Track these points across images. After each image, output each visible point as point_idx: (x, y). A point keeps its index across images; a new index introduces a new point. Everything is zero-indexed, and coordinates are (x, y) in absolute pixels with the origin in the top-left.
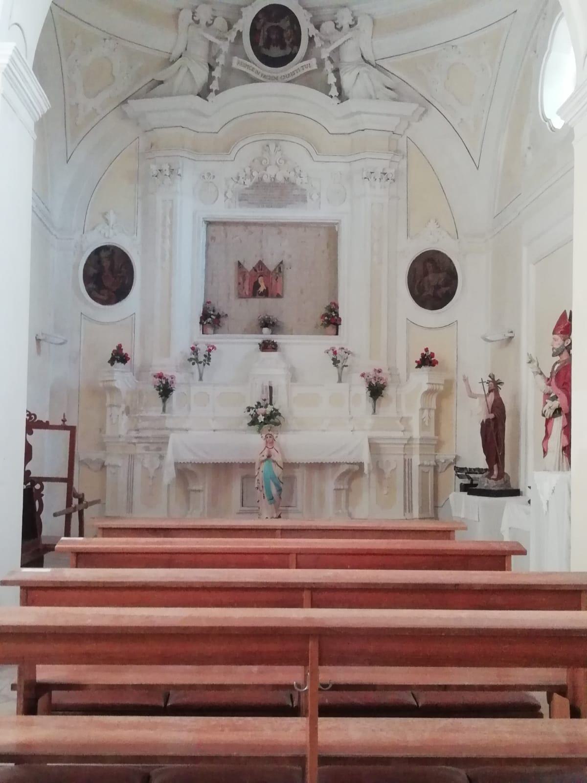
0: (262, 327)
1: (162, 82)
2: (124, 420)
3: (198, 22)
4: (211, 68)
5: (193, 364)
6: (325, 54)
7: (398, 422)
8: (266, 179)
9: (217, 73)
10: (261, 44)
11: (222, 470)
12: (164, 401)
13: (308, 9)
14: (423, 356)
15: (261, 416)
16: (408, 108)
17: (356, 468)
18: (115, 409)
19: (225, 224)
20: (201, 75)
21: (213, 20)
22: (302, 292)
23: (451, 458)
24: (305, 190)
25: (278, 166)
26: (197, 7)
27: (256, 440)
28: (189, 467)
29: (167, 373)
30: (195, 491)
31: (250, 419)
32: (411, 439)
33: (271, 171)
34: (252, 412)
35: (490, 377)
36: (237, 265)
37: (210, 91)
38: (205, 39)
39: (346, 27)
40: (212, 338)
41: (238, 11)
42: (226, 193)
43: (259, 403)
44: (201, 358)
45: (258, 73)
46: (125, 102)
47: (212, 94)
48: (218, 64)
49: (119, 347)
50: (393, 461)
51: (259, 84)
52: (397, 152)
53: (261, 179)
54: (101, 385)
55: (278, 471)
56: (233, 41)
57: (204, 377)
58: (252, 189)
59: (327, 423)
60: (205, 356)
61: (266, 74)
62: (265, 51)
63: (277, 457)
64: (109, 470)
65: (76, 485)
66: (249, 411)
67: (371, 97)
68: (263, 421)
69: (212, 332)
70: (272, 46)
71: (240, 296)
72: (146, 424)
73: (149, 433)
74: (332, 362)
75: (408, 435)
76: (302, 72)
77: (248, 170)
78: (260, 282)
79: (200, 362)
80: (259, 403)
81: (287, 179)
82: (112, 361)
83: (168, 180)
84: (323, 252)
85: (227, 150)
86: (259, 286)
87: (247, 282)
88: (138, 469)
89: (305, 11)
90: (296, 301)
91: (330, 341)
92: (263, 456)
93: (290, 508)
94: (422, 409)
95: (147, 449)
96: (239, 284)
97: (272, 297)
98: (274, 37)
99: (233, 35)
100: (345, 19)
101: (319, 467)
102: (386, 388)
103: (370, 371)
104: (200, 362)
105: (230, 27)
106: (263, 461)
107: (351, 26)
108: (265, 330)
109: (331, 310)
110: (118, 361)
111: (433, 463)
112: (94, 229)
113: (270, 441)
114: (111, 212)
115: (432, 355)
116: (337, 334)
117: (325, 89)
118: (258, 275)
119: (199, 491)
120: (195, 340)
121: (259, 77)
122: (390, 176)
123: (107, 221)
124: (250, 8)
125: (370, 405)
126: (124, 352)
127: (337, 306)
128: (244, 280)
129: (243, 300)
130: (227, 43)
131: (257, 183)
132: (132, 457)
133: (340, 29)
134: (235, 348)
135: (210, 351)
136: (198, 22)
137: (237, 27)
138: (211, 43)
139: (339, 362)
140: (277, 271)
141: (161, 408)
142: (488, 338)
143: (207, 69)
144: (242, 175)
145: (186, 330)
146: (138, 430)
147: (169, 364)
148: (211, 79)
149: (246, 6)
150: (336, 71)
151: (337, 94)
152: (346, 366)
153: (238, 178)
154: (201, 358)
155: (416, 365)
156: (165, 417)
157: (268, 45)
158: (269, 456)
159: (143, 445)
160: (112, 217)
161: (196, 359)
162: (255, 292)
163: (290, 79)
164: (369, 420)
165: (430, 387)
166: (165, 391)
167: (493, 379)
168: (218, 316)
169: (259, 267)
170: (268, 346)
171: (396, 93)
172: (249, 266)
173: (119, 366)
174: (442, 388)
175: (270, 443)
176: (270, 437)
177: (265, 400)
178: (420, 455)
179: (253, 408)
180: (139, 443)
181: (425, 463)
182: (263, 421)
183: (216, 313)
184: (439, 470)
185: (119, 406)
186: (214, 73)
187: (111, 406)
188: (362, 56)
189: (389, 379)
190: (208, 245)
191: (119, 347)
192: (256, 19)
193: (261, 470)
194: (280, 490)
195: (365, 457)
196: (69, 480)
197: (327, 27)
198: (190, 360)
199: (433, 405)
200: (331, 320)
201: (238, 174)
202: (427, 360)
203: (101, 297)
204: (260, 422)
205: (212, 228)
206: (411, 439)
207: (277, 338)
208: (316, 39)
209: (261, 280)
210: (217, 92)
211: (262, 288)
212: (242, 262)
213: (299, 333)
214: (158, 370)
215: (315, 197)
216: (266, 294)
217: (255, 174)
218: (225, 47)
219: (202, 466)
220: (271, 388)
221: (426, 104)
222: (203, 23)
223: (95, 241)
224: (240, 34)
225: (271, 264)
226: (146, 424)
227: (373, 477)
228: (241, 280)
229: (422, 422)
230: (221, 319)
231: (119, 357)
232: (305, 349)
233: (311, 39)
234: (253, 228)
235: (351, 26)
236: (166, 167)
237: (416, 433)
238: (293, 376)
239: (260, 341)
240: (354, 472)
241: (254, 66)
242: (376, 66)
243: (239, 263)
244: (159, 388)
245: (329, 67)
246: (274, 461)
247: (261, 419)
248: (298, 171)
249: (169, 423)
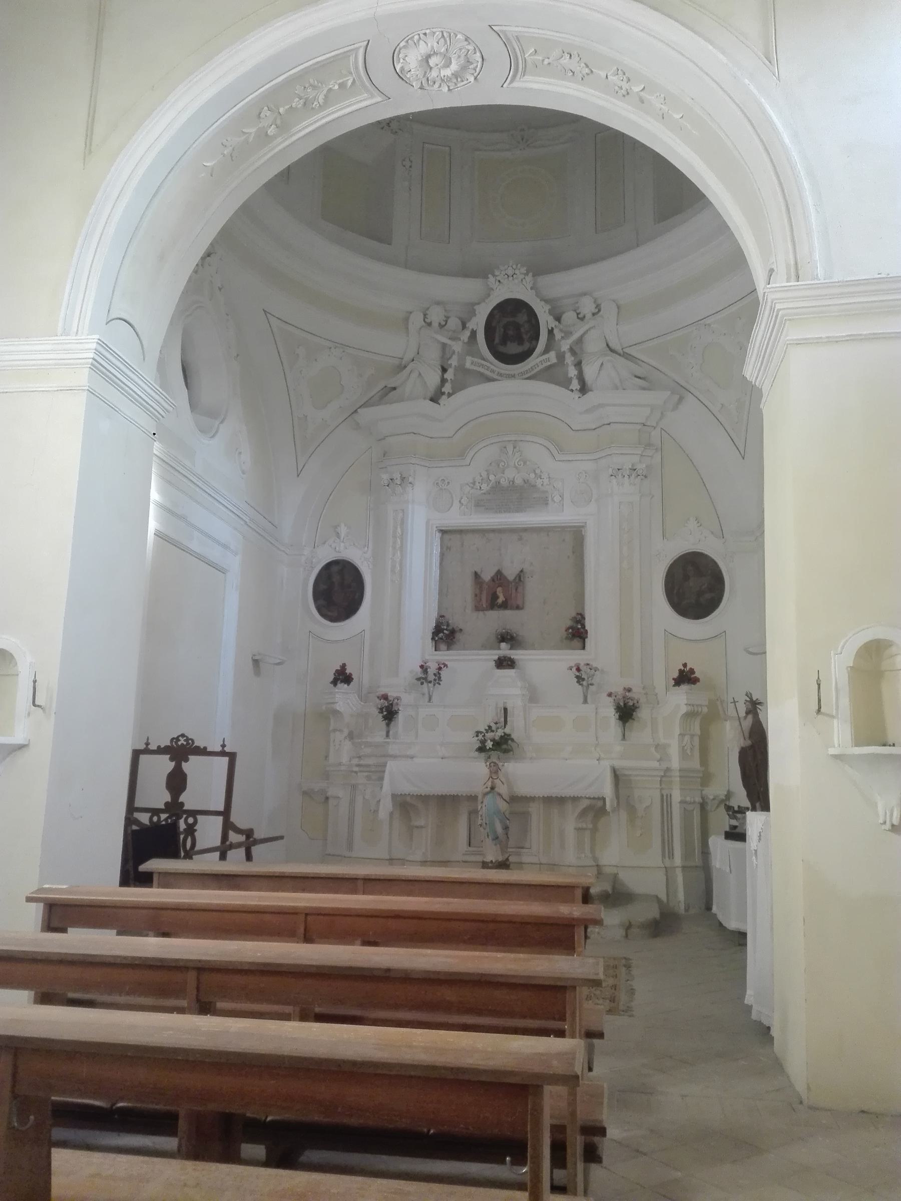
1: (395, 389)
2: (347, 745)
3: (430, 324)
4: (444, 370)
5: (422, 684)
6: (565, 346)
7: (653, 749)
8: (504, 482)
9: (449, 375)
10: (497, 341)
11: (446, 803)
12: (388, 725)
13: (547, 301)
14: (681, 672)
16: (658, 397)
17: (600, 803)
18: (337, 733)
19: (461, 532)
20: (433, 378)
21: (446, 322)
23: (722, 793)
25: (516, 468)
26: (428, 309)
27: (480, 768)
28: (408, 799)
29: (392, 694)
30: (417, 827)
31: (478, 745)
32: (668, 770)
33: (510, 474)
34: (480, 737)
35: (747, 695)
37: (443, 394)
38: (438, 342)
39: (589, 316)
40: (444, 655)
41: (470, 309)
43: (490, 727)
44: (431, 677)
45: (493, 371)
46: (356, 411)
47: (444, 397)
48: (450, 365)
49: (344, 666)
50: (648, 796)
51: (492, 383)
52: (649, 445)
54: (324, 707)
55: (503, 806)
56: (466, 340)
57: (434, 698)
59: (568, 751)
60: (435, 674)
61: (502, 372)
62: (502, 349)
63: (502, 789)
64: (331, 801)
65: (234, 818)
66: (477, 736)
67: (617, 388)
70: (509, 343)
71: (478, 608)
72: (368, 751)
73: (371, 761)
74: (576, 680)
75: (664, 765)
76: (541, 367)
77: (484, 474)
78: (498, 592)
79: (430, 682)
80: (490, 727)
82: (335, 682)
83: (399, 489)
85: (462, 455)
86: (498, 597)
88: (359, 800)
89: (543, 303)
90: (537, 614)
91: (575, 656)
93: (524, 850)
94: (682, 735)
95: (368, 778)
96: (476, 595)
97: (512, 608)
98: (511, 333)
99: (467, 333)
100: (587, 307)
101: (561, 801)
102: (638, 710)
103: (619, 690)
105: (464, 326)
106: (487, 794)
107: (594, 314)
108: (503, 645)
109: (578, 622)
110: (342, 682)
111: (698, 799)
112: (324, 543)
113: (495, 771)
114: (343, 525)
115: (692, 671)
117: (565, 383)
119: (422, 827)
120: (427, 657)
121: (495, 377)
122: (640, 472)
123: (338, 535)
124: (483, 304)
125: (620, 730)
126: (348, 671)
127: (584, 618)
129: (481, 613)
130: (460, 343)
132: (354, 787)
133: (582, 319)
134: (469, 666)
135: (440, 669)
136: (430, 324)
137: (471, 325)
138: (444, 346)
139: (583, 679)
141: (384, 733)
142: (750, 650)
143: (440, 372)
144: (478, 479)
145: (416, 646)
146: (360, 757)
147: (397, 684)
148: (443, 381)
149: (479, 304)
150: (578, 365)
151: (578, 387)
152: (592, 684)
153: (474, 483)
154: (431, 677)
155: (673, 682)
156: (388, 743)
157: (504, 342)
158: (492, 788)
159: (366, 774)
160: (343, 530)
161: (425, 679)
162: (493, 604)
163: (527, 376)
164: (618, 748)
165: (690, 708)
166: (389, 713)
167: (751, 699)
168: (453, 632)
170: (504, 663)
171: (646, 382)
172: (487, 577)
173: (342, 687)
174: (705, 710)
178: (681, 789)
179: (481, 732)
180: (361, 771)
181: (688, 799)
183: (450, 628)
184: (709, 808)
185: (340, 731)
186: (446, 376)
187: (335, 730)
188: (607, 345)
189: (643, 700)
190: (442, 556)
191: (344, 666)
192: (491, 316)
194: (506, 828)
195: (607, 790)
196: (226, 813)
197: (569, 317)
198: (418, 679)
199: (697, 730)
200: (577, 633)
201: (474, 479)
202: (685, 677)
203: (329, 614)
205: (447, 537)
206: (668, 770)
207: (516, 654)
208: (556, 331)
209: (500, 592)
210: (449, 395)
211: (501, 599)
212: (479, 572)
213: (542, 648)
214: (383, 691)
215: (557, 498)
216: (505, 606)
217: (492, 477)
218: (457, 347)
219: (425, 799)
220: (505, 710)
221: (680, 392)
222: (435, 325)
223: (325, 556)
224: (474, 334)
225: (510, 574)
226: (368, 751)
227: (624, 815)
229: (683, 750)
230: (458, 635)
231: (343, 677)
232: (547, 665)
233: (551, 332)
235: (594, 314)
236: (397, 476)
237: (675, 763)
238: (533, 696)
239: (496, 657)
240: (596, 810)
241: (488, 364)
242: (626, 356)
243: (476, 573)
244: (381, 710)
245: (569, 359)
246: (499, 794)
248: (538, 471)
249: (392, 749)
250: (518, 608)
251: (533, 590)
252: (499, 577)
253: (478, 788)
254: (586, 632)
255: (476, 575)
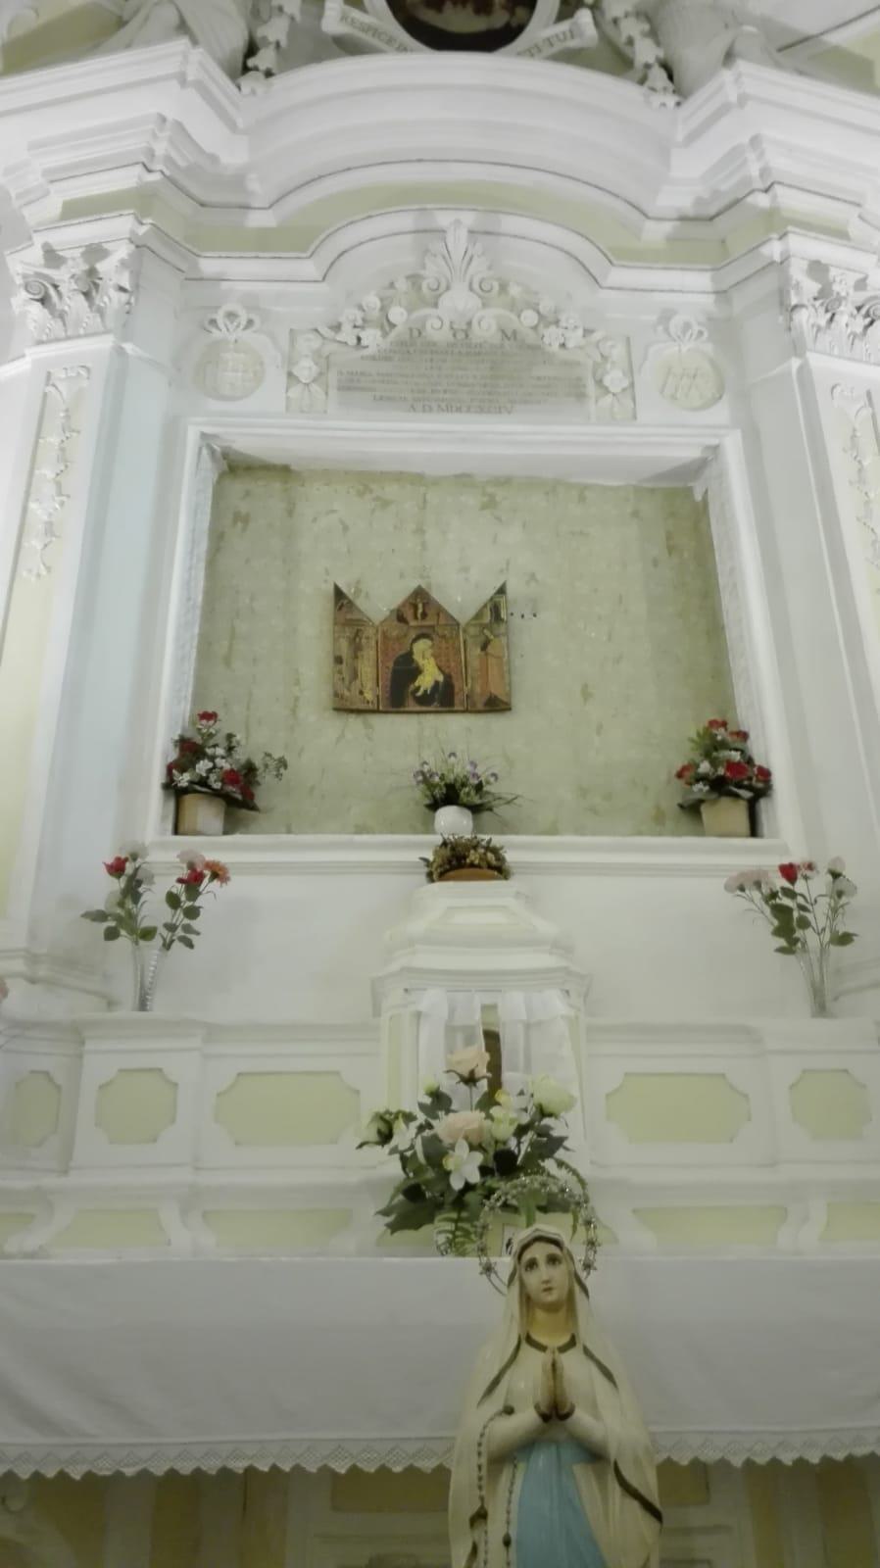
0: (435, 806)
5: (111, 935)
8: (437, 330)
15: (462, 1150)
22: (586, 694)
24: (578, 364)
33: (459, 301)
36: (330, 605)
42: (290, 361)
44: (153, 909)
53: (417, 332)
58: (387, 359)
60: (173, 900)
62: (429, 16)
63: (607, 1416)
66: (385, 1137)
68: (475, 1178)
69: (218, 823)
71: (343, 707)
77: (372, 301)
78: (421, 661)
79: (148, 934)
81: (509, 335)
84: (655, 563)
86: (417, 671)
87: (369, 655)
92: (509, 1411)
96: (338, 660)
104: (148, 934)
106: (523, 1448)
116: (754, 831)
118: (413, 635)
128: (356, 649)
129: (355, 722)
131: (403, 343)
140: (487, 618)
153: (337, 328)
158: (555, 1413)
162: (400, 691)
169: (416, 608)
172: (380, 601)
175: (552, 1308)
176: (553, 1260)
177: (470, 1080)
182: (475, 1178)
193: (496, 1528)
200: (726, 780)
204: (457, 1184)
205: (237, 487)
209: (423, 652)
211: (429, 678)
215: (615, 379)
216: (443, 698)
217: (397, 314)
225: (460, 598)
228: (345, 650)
234: (391, 490)
243: (339, 594)
246: (594, 1455)
247: (465, 1167)
250: (496, 705)
251: (542, 659)
252: (420, 609)
253: (466, 1420)
254: (765, 774)
255: (340, 598)
